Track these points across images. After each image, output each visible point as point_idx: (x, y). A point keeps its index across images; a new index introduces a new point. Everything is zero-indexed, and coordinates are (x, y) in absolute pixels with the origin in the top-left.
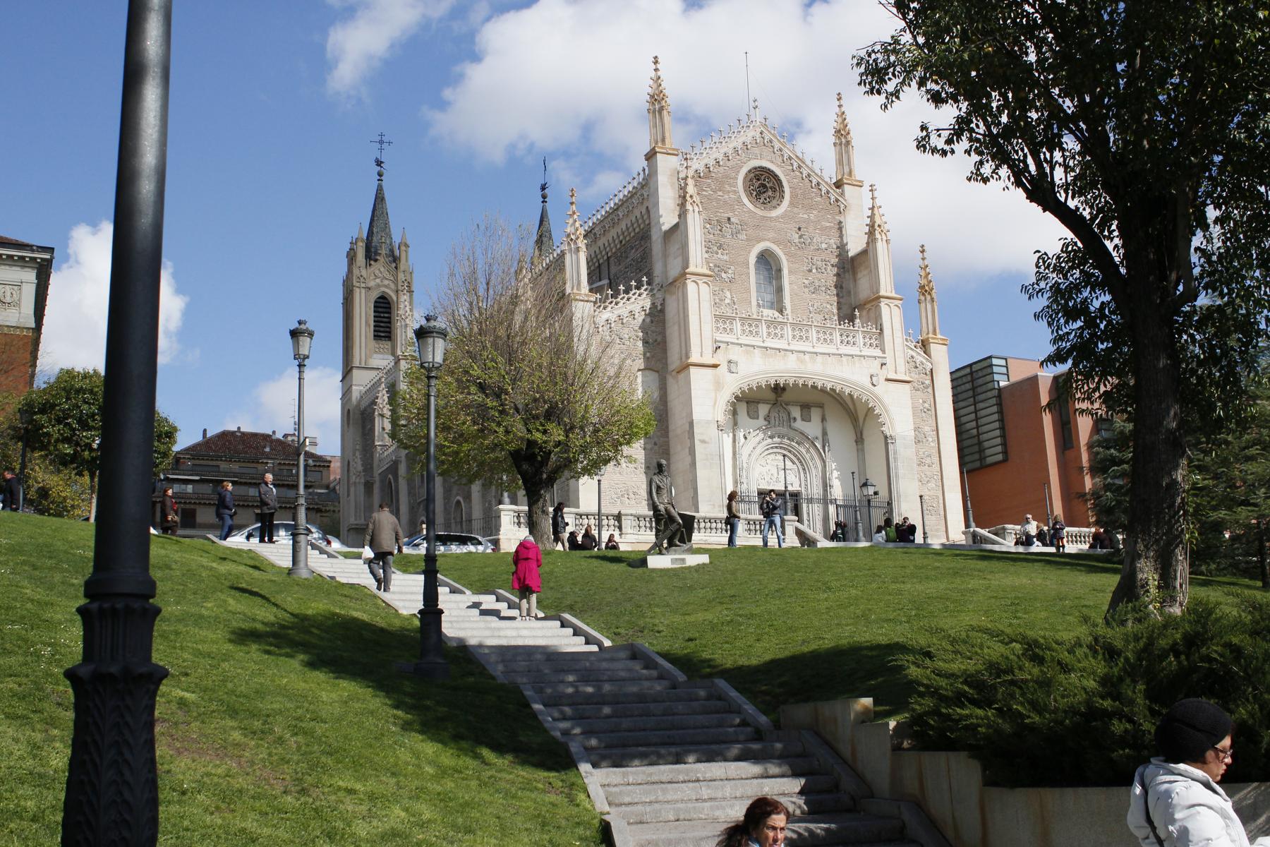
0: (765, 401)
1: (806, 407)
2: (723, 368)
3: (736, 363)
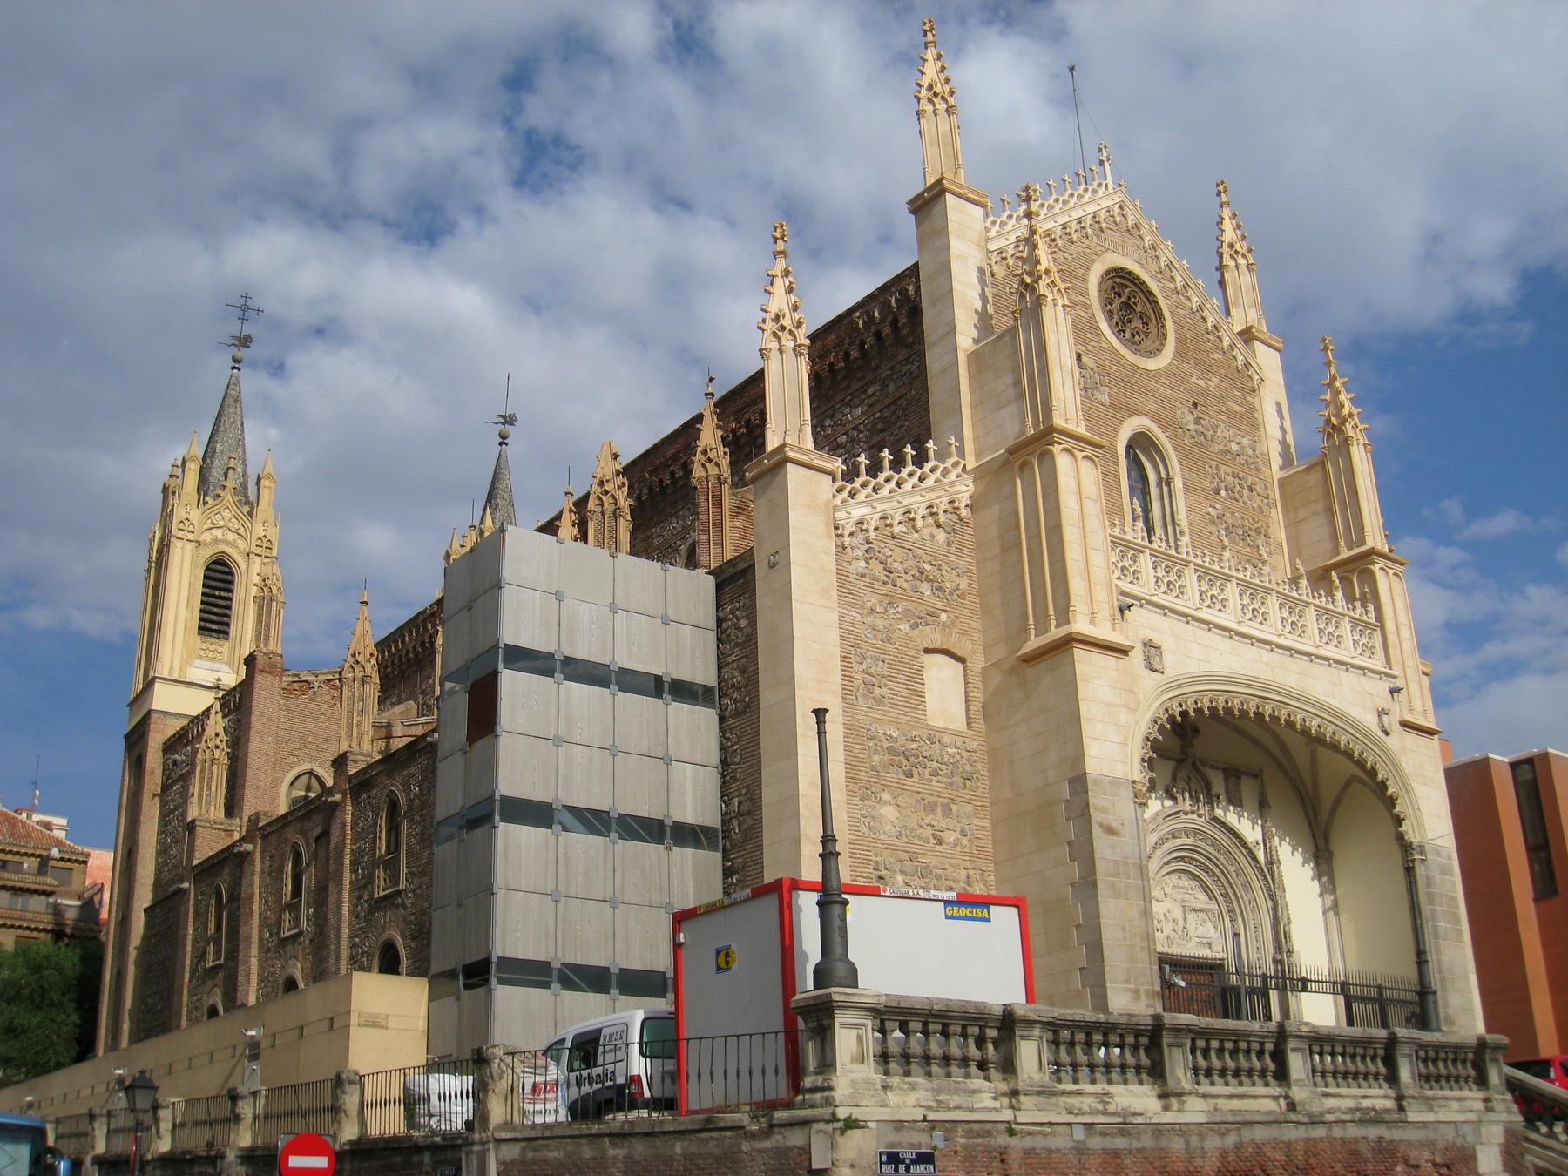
2: (1137, 656)
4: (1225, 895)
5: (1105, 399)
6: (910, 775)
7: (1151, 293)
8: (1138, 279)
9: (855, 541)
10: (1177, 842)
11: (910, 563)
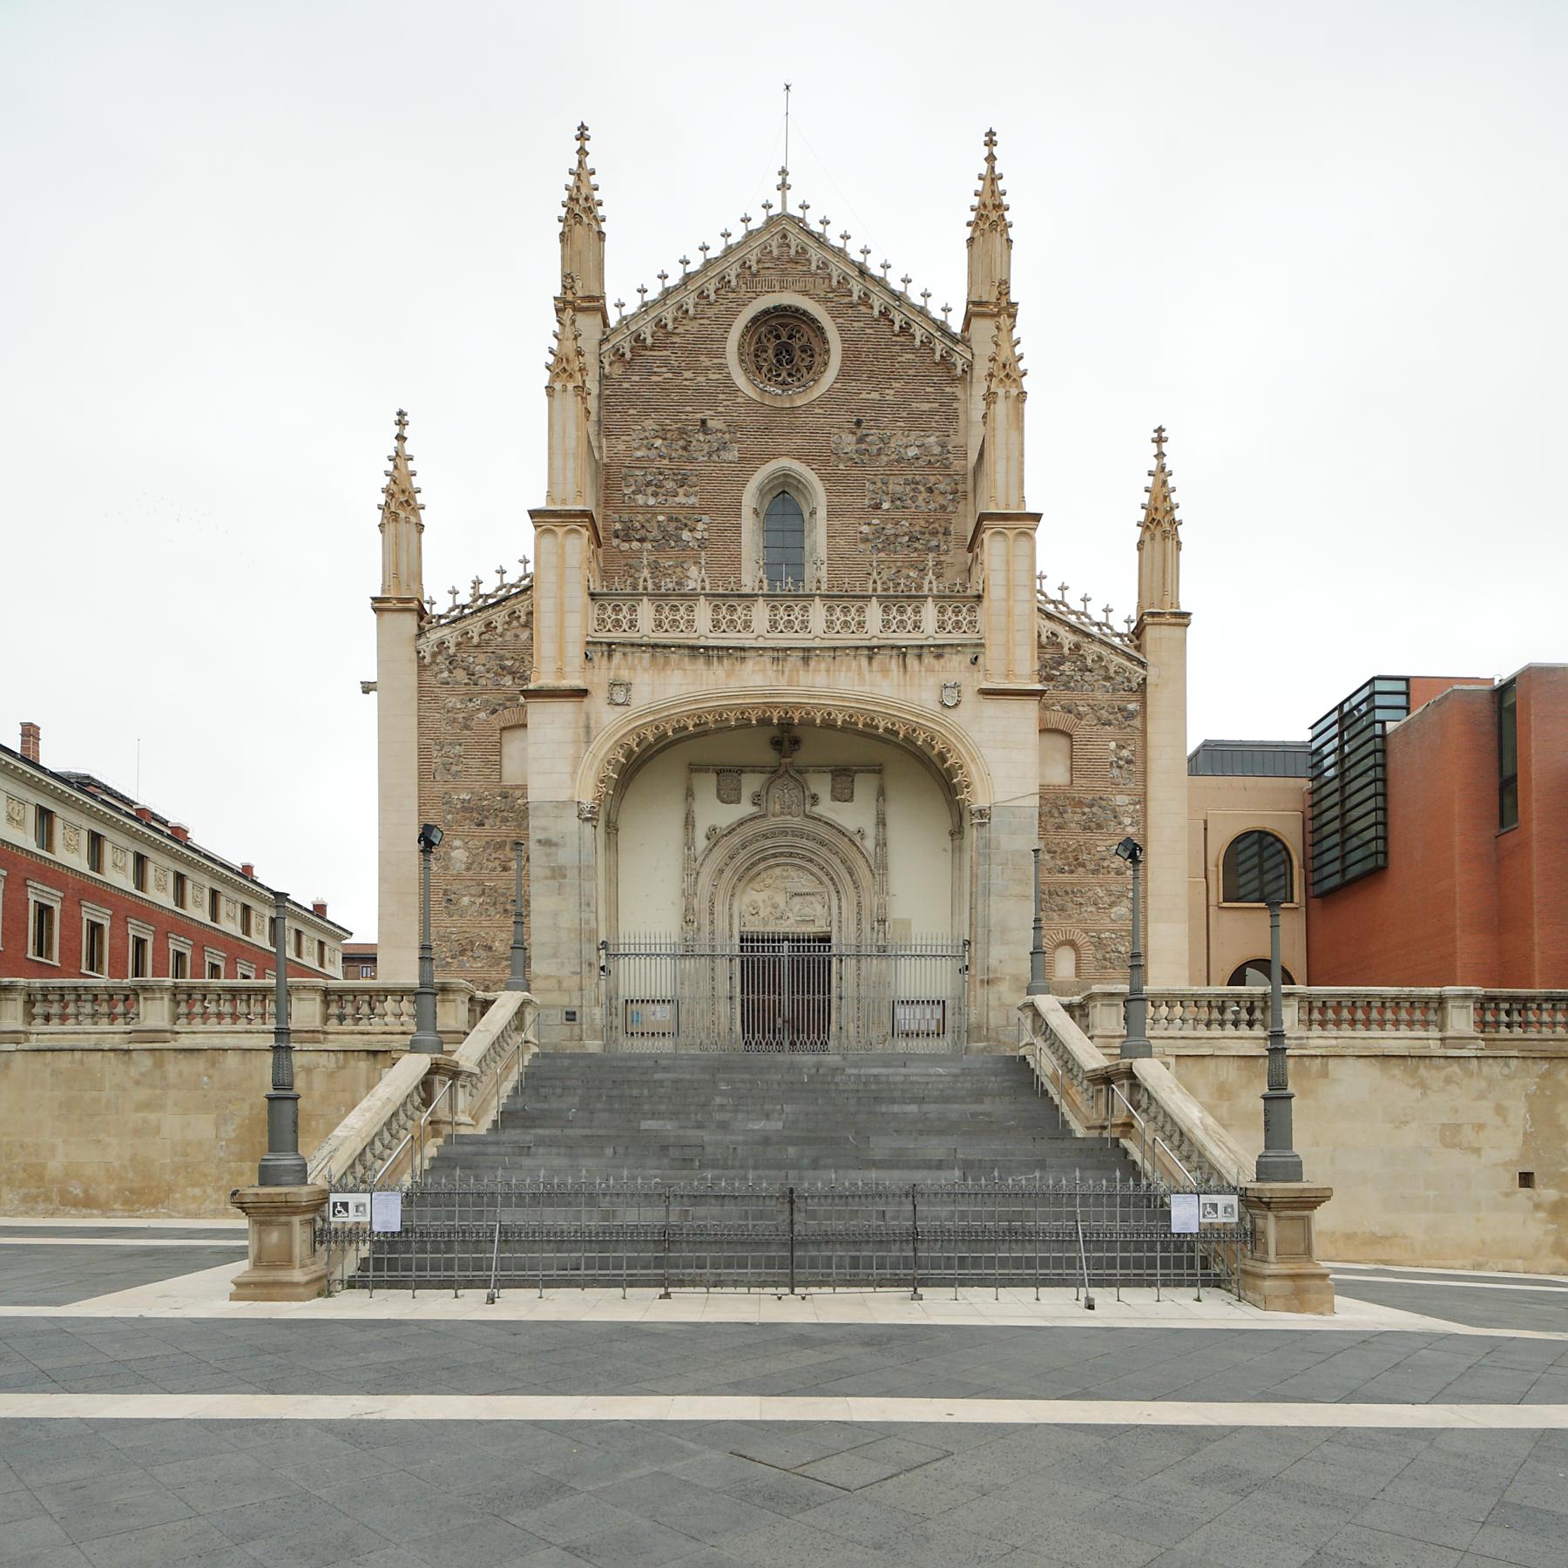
0: (755, 769)
1: (843, 777)
5: (733, 455)
7: (814, 320)
8: (797, 310)
9: (440, 659)
10: (768, 843)
11: (493, 664)
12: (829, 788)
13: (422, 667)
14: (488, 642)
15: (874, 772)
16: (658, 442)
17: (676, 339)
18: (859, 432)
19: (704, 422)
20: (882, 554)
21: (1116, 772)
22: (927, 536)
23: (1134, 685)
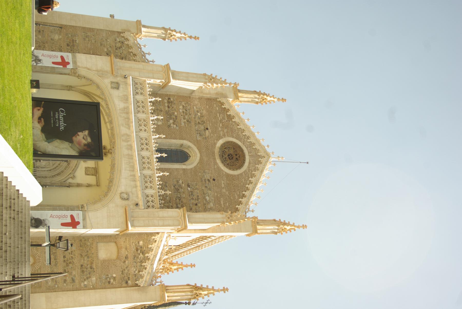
3: (118, 88)
4: (55, 168)
6: (68, 45)
12: (90, 166)
13: (119, 33)
14: (130, 54)
15: (97, 183)
16: (199, 114)
17: (231, 122)
18: (211, 180)
19: (207, 129)
20: (173, 187)
21: (104, 277)
22: (181, 204)
23: (137, 282)
